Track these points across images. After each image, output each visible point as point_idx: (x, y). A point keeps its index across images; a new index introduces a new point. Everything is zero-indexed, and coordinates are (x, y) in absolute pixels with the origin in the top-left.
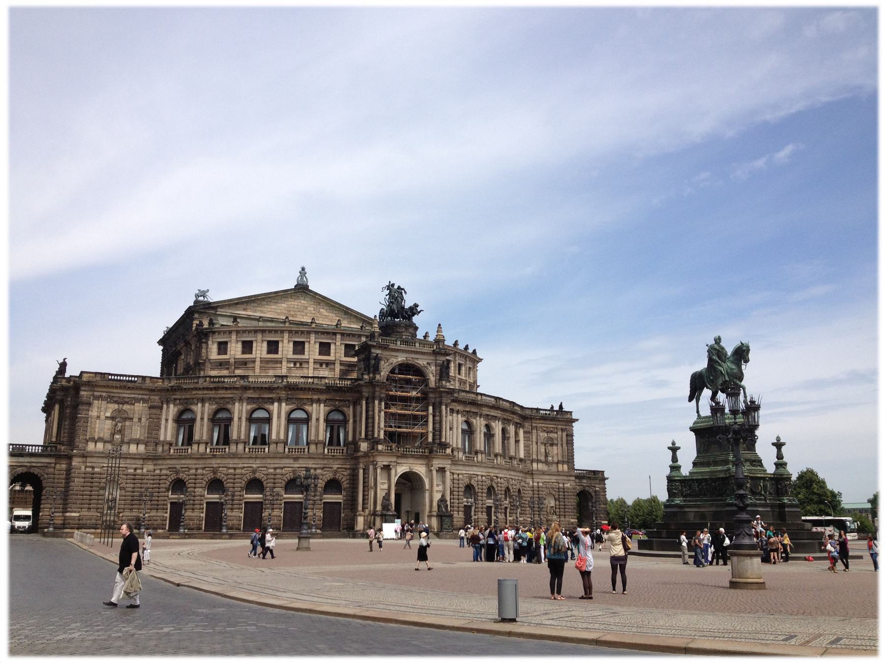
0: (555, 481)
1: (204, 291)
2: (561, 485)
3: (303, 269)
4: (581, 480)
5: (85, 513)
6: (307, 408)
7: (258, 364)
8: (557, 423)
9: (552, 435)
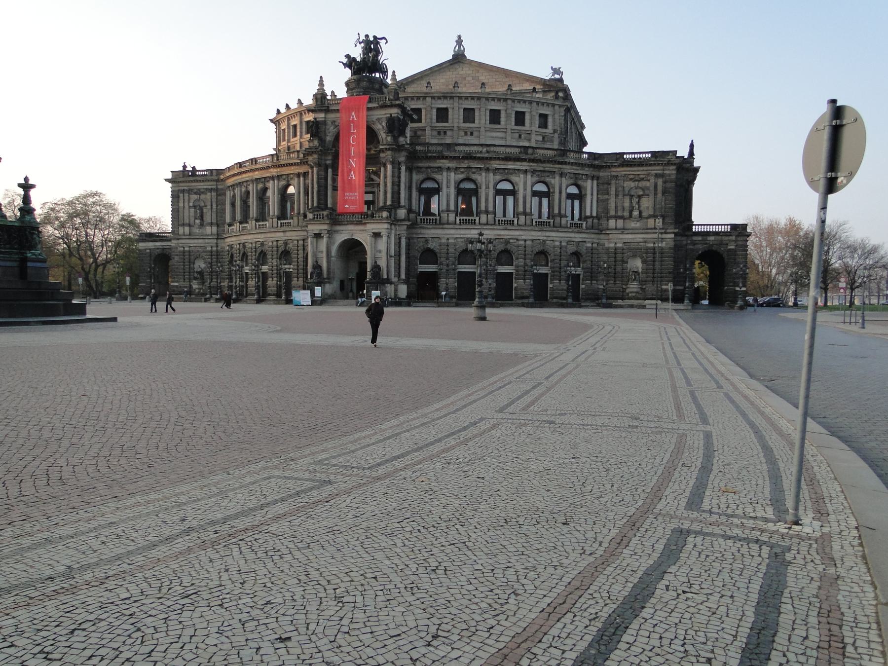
0: (641, 240)
2: (651, 245)
3: (459, 37)
4: (705, 237)
5: (182, 283)
7: (299, 145)
8: (650, 168)
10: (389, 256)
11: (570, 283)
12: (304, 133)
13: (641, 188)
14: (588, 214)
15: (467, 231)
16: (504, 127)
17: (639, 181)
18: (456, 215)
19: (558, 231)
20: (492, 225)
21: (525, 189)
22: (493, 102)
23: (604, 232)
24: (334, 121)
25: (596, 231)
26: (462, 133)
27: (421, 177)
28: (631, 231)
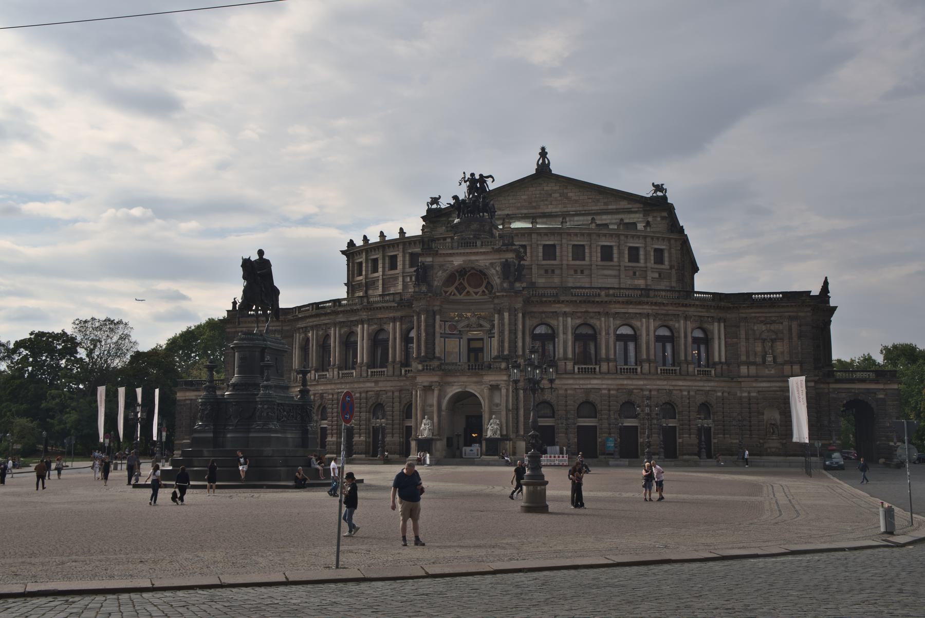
1: (435, 198)
3: (543, 149)
6: (385, 327)
7: (381, 282)
9: (774, 327)
10: (507, 410)
11: (703, 437)
12: (387, 269)
13: (773, 331)
14: (717, 359)
15: (588, 382)
16: (617, 264)
17: (771, 324)
18: (575, 364)
19: (685, 380)
20: (613, 374)
21: (648, 335)
22: (604, 238)
23: (735, 380)
24: (443, 265)
25: (727, 379)
26: (572, 272)
27: (535, 322)
28: (765, 379)
